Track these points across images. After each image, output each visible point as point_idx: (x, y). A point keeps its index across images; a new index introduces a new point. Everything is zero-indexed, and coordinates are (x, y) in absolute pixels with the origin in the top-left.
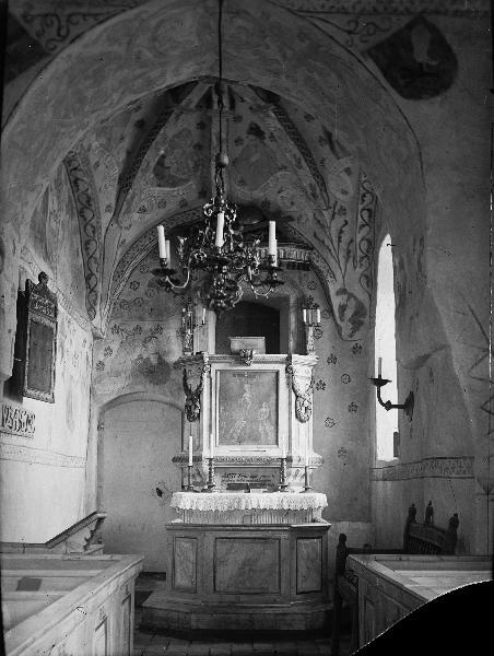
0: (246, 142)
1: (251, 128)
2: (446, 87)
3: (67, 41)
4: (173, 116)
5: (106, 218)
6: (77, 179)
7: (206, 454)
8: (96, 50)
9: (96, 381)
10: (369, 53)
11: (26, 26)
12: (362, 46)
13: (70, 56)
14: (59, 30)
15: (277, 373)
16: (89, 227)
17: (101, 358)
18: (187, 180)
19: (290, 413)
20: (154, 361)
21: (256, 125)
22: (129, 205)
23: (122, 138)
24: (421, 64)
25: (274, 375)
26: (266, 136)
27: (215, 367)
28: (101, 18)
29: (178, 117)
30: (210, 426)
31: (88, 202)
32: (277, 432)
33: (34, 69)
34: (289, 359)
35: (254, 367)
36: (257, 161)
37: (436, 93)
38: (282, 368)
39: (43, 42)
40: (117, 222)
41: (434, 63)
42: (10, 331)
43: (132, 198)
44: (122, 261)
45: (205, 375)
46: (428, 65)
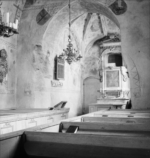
2: (125, 12)
3: (55, 14)
4: (91, 18)
5: (81, 40)
7: (104, 90)
8: (61, 14)
9: (82, 75)
10: (109, 7)
11: (48, 12)
12: (108, 6)
13: (56, 16)
15: (119, 71)
16: (77, 43)
17: (83, 70)
18: (98, 30)
19: (122, 79)
20: (94, 70)
22: (86, 37)
23: (82, 23)
24: (120, 8)
25: (118, 71)
27: (106, 70)
28: (60, 8)
29: (92, 17)
30: (105, 83)
32: (119, 84)
33: (49, 20)
34: (121, 68)
35: (114, 70)
37: (123, 13)
38: (119, 70)
39: (51, 14)
40: (83, 41)
41: (122, 7)
42: (52, 67)
43: (86, 35)
44: (86, 49)
45: (103, 72)
46: (121, 7)
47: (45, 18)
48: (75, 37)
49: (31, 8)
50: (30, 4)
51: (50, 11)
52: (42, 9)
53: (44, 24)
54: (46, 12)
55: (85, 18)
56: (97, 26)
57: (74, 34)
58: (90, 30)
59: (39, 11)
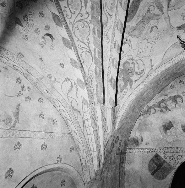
11: (166, 160)
14: (175, 160)
47: (163, 168)
49: (137, 150)
50: (134, 145)
51: (168, 158)
52: (154, 154)
53: (163, 179)
54: (162, 159)
59: (152, 155)
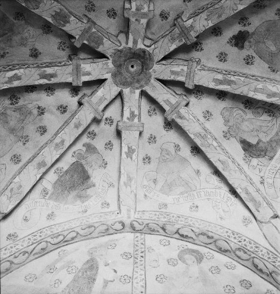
0: (251, 52)
1: (236, 45)
4: (179, 121)
6: (177, 232)
16: (238, 253)
21: (231, 39)
23: (198, 172)
26: (243, 29)
29: (181, 117)
31: (208, 237)
36: (275, 45)
43: (247, 193)
48: (203, 239)
55: (186, 150)
56: (258, 123)
57: (181, 232)
58: (255, 161)
